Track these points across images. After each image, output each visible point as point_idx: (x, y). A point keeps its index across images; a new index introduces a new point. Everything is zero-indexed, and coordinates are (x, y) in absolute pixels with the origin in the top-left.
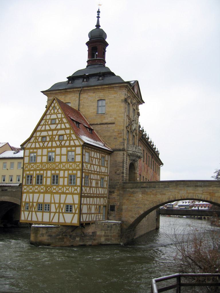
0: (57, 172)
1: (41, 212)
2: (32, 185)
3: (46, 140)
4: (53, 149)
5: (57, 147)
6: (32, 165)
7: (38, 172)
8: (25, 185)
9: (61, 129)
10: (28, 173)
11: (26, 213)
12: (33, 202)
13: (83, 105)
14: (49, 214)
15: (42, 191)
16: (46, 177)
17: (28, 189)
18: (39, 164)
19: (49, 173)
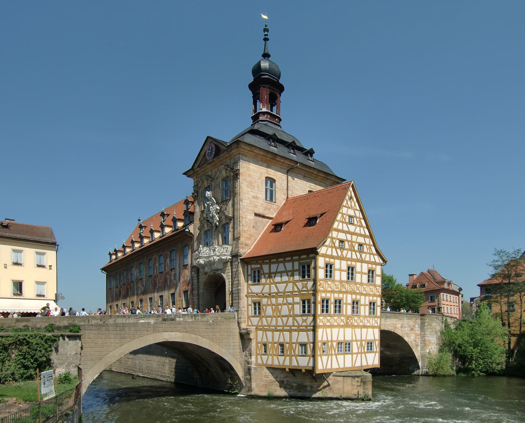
0: (358, 297)
1: (342, 354)
2: (330, 316)
3: (344, 246)
4: (354, 263)
5: (357, 261)
6: (329, 283)
7: (336, 295)
8: (321, 315)
9: (361, 235)
10: (323, 295)
11: (325, 358)
12: (332, 341)
13: (292, 191)
14: (350, 356)
15: (342, 324)
16: (347, 304)
17: (325, 320)
18: (338, 283)
19: (349, 296)
